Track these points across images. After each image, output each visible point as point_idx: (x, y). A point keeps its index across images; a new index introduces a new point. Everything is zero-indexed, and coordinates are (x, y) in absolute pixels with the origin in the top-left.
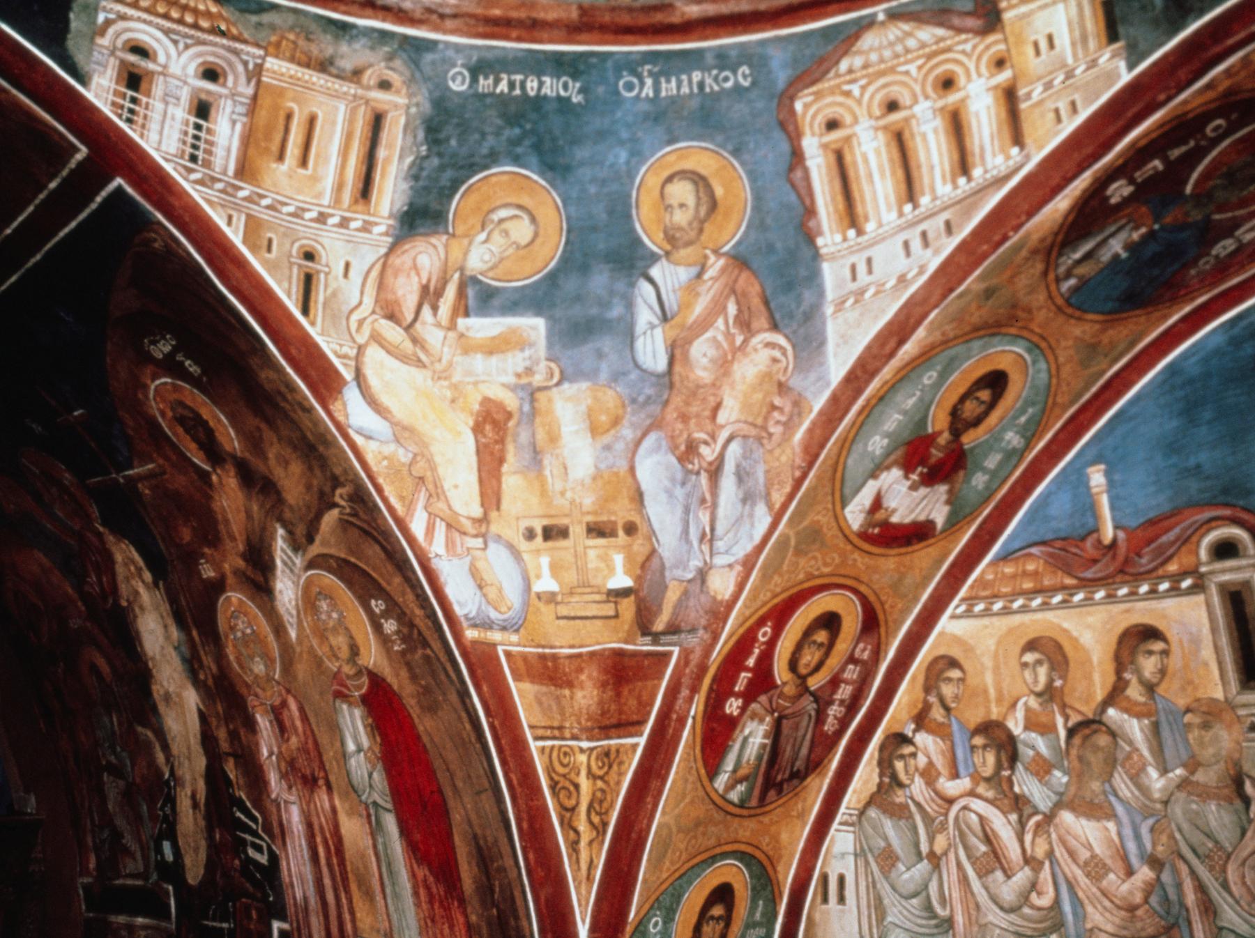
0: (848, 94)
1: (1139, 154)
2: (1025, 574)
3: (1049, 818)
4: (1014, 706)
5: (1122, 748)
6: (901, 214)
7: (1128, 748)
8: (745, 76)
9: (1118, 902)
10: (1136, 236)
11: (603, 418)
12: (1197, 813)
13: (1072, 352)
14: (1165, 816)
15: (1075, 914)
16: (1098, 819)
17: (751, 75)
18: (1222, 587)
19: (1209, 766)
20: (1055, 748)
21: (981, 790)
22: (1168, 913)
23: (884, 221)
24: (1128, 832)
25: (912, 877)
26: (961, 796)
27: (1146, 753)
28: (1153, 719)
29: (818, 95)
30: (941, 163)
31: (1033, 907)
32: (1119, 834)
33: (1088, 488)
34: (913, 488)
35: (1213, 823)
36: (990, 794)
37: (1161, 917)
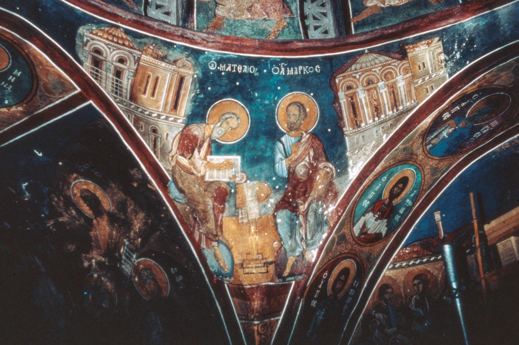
0: (355, 77)
1: (453, 104)
6: (374, 121)
8: (318, 69)
10: (450, 131)
11: (262, 195)
13: (429, 170)
17: (320, 69)
23: (368, 123)
29: (344, 77)
30: (388, 103)
33: (434, 220)
34: (376, 220)
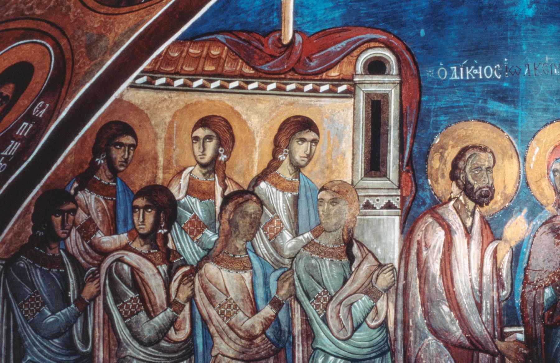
2: (208, 57)
3: (196, 269)
4: (180, 173)
5: (266, 215)
7: (271, 216)
9: (241, 334)
12: (315, 267)
14: (291, 268)
15: (205, 344)
16: (237, 271)
18: (368, 95)
19: (330, 232)
20: (210, 212)
21: (136, 245)
22: (279, 341)
24: (260, 280)
25: (56, 321)
26: (116, 250)
27: (285, 220)
28: (295, 194)
31: (170, 341)
32: (253, 283)
35: (325, 275)
36: (145, 249)
37: (273, 343)
